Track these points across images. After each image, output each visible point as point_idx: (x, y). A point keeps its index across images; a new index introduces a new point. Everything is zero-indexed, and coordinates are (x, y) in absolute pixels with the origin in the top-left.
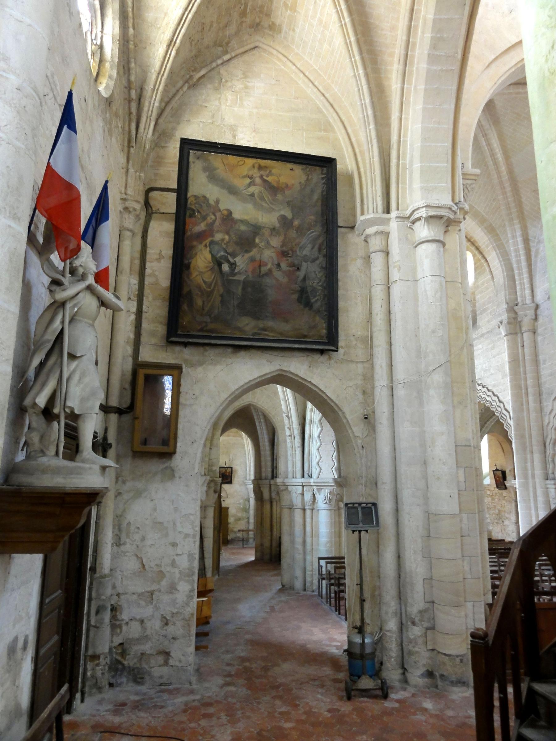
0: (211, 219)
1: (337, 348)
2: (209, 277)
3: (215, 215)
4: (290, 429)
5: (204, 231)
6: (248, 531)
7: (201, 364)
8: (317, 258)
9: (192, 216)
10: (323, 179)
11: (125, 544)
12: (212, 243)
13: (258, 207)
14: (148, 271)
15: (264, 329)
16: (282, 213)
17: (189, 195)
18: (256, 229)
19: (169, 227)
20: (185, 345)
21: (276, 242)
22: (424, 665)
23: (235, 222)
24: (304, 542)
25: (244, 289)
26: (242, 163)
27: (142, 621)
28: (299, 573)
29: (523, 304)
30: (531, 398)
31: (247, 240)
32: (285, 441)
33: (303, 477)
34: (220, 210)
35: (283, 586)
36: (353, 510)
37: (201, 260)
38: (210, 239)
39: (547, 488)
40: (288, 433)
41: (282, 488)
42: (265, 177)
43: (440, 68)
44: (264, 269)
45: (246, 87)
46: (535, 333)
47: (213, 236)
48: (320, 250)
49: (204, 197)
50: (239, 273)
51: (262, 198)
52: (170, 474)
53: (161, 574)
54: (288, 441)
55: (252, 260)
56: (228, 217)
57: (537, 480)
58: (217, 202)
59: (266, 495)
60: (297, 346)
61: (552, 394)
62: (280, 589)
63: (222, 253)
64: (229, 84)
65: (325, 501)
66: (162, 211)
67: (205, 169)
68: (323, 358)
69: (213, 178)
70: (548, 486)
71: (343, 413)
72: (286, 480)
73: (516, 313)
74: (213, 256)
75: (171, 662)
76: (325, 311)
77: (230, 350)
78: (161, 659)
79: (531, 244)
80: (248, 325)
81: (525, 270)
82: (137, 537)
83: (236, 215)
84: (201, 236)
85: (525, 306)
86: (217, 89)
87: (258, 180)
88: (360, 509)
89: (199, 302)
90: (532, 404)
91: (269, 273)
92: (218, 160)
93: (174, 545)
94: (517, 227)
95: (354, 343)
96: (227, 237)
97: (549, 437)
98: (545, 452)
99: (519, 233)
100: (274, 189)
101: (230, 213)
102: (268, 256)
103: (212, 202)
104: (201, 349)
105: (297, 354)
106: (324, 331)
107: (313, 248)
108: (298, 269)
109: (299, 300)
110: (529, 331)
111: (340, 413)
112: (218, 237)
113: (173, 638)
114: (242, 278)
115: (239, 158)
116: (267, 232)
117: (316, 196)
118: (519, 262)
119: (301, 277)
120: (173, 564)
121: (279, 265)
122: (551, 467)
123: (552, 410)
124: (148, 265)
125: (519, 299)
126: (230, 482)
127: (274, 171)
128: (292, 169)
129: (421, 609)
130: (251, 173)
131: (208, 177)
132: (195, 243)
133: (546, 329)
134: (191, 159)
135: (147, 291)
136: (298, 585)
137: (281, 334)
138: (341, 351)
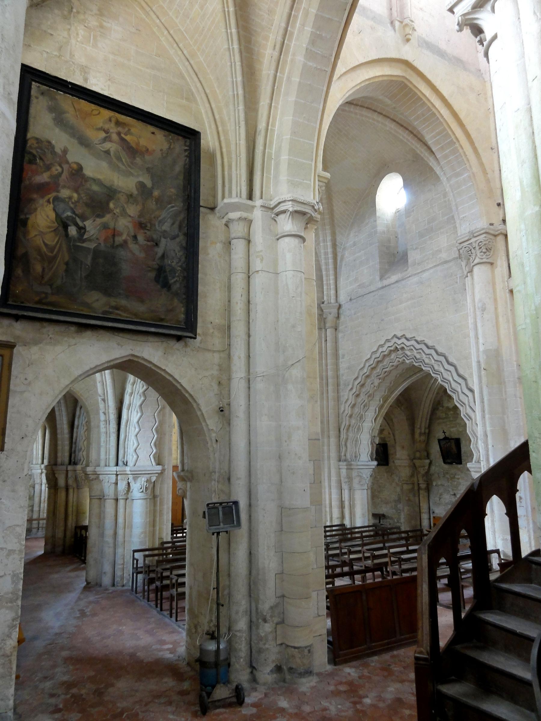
0: (57, 170)
1: (196, 335)
2: (51, 239)
3: (60, 166)
4: (105, 414)
5: (47, 184)
7: (36, 342)
8: (178, 236)
9: (32, 161)
10: (186, 150)
12: (56, 199)
15: (117, 308)
16: (141, 179)
17: (29, 135)
18: (111, 193)
20: (17, 318)
21: (133, 210)
22: (273, 661)
23: (86, 179)
24: (115, 534)
25: (94, 259)
26: (97, 112)
28: (107, 568)
29: (328, 303)
30: (330, 388)
31: (100, 202)
32: (99, 427)
33: (117, 464)
34: (67, 162)
35: (88, 583)
36: (213, 511)
39: (340, 469)
40: (102, 417)
41: (92, 477)
42: (123, 135)
43: (315, 66)
44: (119, 240)
45: (101, 26)
46: (336, 330)
47: (58, 191)
48: (180, 227)
49: (49, 142)
50: (89, 240)
51: (119, 159)
56: (77, 172)
57: (332, 462)
58: (65, 151)
59: (61, 482)
60: (153, 330)
61: (348, 385)
62: (85, 588)
63: (69, 214)
64: (81, 17)
65: (142, 490)
67: (51, 109)
68: (178, 345)
69: (60, 121)
70: (340, 467)
71: (198, 405)
72: (98, 469)
73: (322, 311)
74: (57, 215)
76: (184, 294)
77: (73, 329)
79: (338, 250)
80: (97, 301)
81: (331, 272)
83: (88, 172)
84: (43, 189)
85: (330, 305)
87: (115, 137)
88: (220, 509)
89: (38, 268)
90: (331, 394)
92: (66, 102)
94: (328, 232)
95: (211, 331)
96: (75, 195)
97: (344, 423)
98: (339, 436)
99: (329, 238)
100: (133, 151)
102: (124, 224)
103: (58, 150)
104: (37, 325)
105: (151, 339)
106: (182, 316)
107: (173, 224)
108: (157, 244)
109: (157, 279)
110: (332, 327)
111: (195, 405)
114: (92, 246)
115: (93, 106)
116: (123, 198)
117: (178, 168)
118: (327, 264)
119: (160, 254)
121: (135, 237)
122: (344, 449)
123: (348, 399)
125: (325, 298)
127: (133, 130)
128: (153, 133)
129: (272, 605)
130: (106, 127)
131: (54, 119)
132: (35, 196)
133: (346, 327)
136: (106, 580)
137: (136, 315)
138: (199, 338)
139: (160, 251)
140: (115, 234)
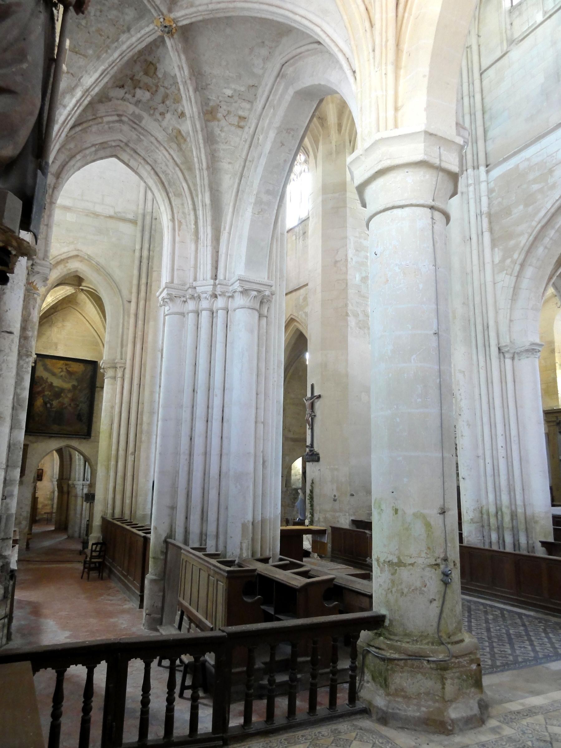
2: (41, 409)
6: (51, 513)
7: (36, 442)
12: (44, 396)
13: (64, 381)
18: (62, 390)
20: (30, 435)
21: (70, 395)
32: (76, 461)
45: (63, 326)
51: (66, 377)
54: (77, 461)
55: (59, 402)
58: (47, 378)
59: (65, 489)
63: (47, 400)
67: (43, 365)
68: (84, 441)
69: (46, 369)
72: (75, 482)
80: (55, 428)
83: (55, 384)
84: (39, 393)
86: (50, 326)
87: (65, 370)
91: (66, 408)
92: (48, 362)
101: (52, 383)
102: (66, 401)
103: (45, 379)
112: (46, 393)
114: (54, 410)
117: (88, 377)
121: (70, 405)
138: (92, 438)
139: (79, 408)
140: (63, 404)
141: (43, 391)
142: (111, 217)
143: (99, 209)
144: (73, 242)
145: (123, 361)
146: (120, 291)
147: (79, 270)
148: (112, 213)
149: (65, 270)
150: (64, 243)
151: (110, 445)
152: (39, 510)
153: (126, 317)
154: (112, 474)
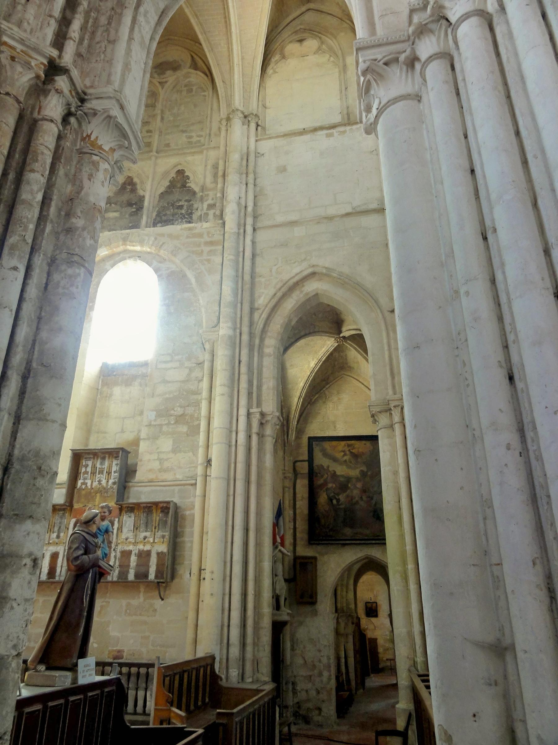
9: (316, 476)
11: (296, 649)
12: (327, 489)
13: (349, 467)
14: (297, 506)
15: (357, 533)
16: (362, 469)
18: (349, 479)
19: (306, 482)
20: (318, 544)
21: (359, 485)
23: (338, 476)
27: (307, 691)
31: (344, 487)
34: (330, 471)
37: (323, 499)
38: (326, 488)
44: (354, 501)
45: (339, 399)
49: (322, 465)
50: (342, 504)
51: (351, 462)
52: (315, 613)
53: (314, 666)
55: (348, 496)
56: (334, 475)
58: (328, 467)
60: (374, 542)
63: (332, 494)
64: (330, 399)
66: (302, 472)
69: (325, 454)
74: (328, 496)
75: (322, 714)
77: (340, 545)
78: (317, 712)
80: (348, 531)
82: (302, 646)
83: (338, 473)
84: (321, 486)
86: (324, 402)
87: (348, 453)
89: (323, 521)
91: (357, 502)
92: (327, 445)
93: (320, 651)
100: (355, 456)
101: (335, 472)
102: (356, 493)
103: (325, 467)
105: (375, 546)
109: (374, 516)
112: (330, 485)
113: (323, 701)
115: (337, 442)
116: (354, 480)
120: (320, 661)
121: (361, 498)
124: (297, 503)
126: (376, 616)
127: (356, 446)
134: (314, 446)
135: (298, 517)
139: (373, 502)
140: (352, 498)
141: (325, 483)
142: (348, 215)
143: (331, 211)
144: (305, 259)
145: (397, 396)
146: (376, 302)
147: (319, 292)
148: (349, 210)
149: (301, 296)
150: (295, 263)
151: (402, 536)
152: (380, 656)
153: (391, 334)
154: (413, 587)
